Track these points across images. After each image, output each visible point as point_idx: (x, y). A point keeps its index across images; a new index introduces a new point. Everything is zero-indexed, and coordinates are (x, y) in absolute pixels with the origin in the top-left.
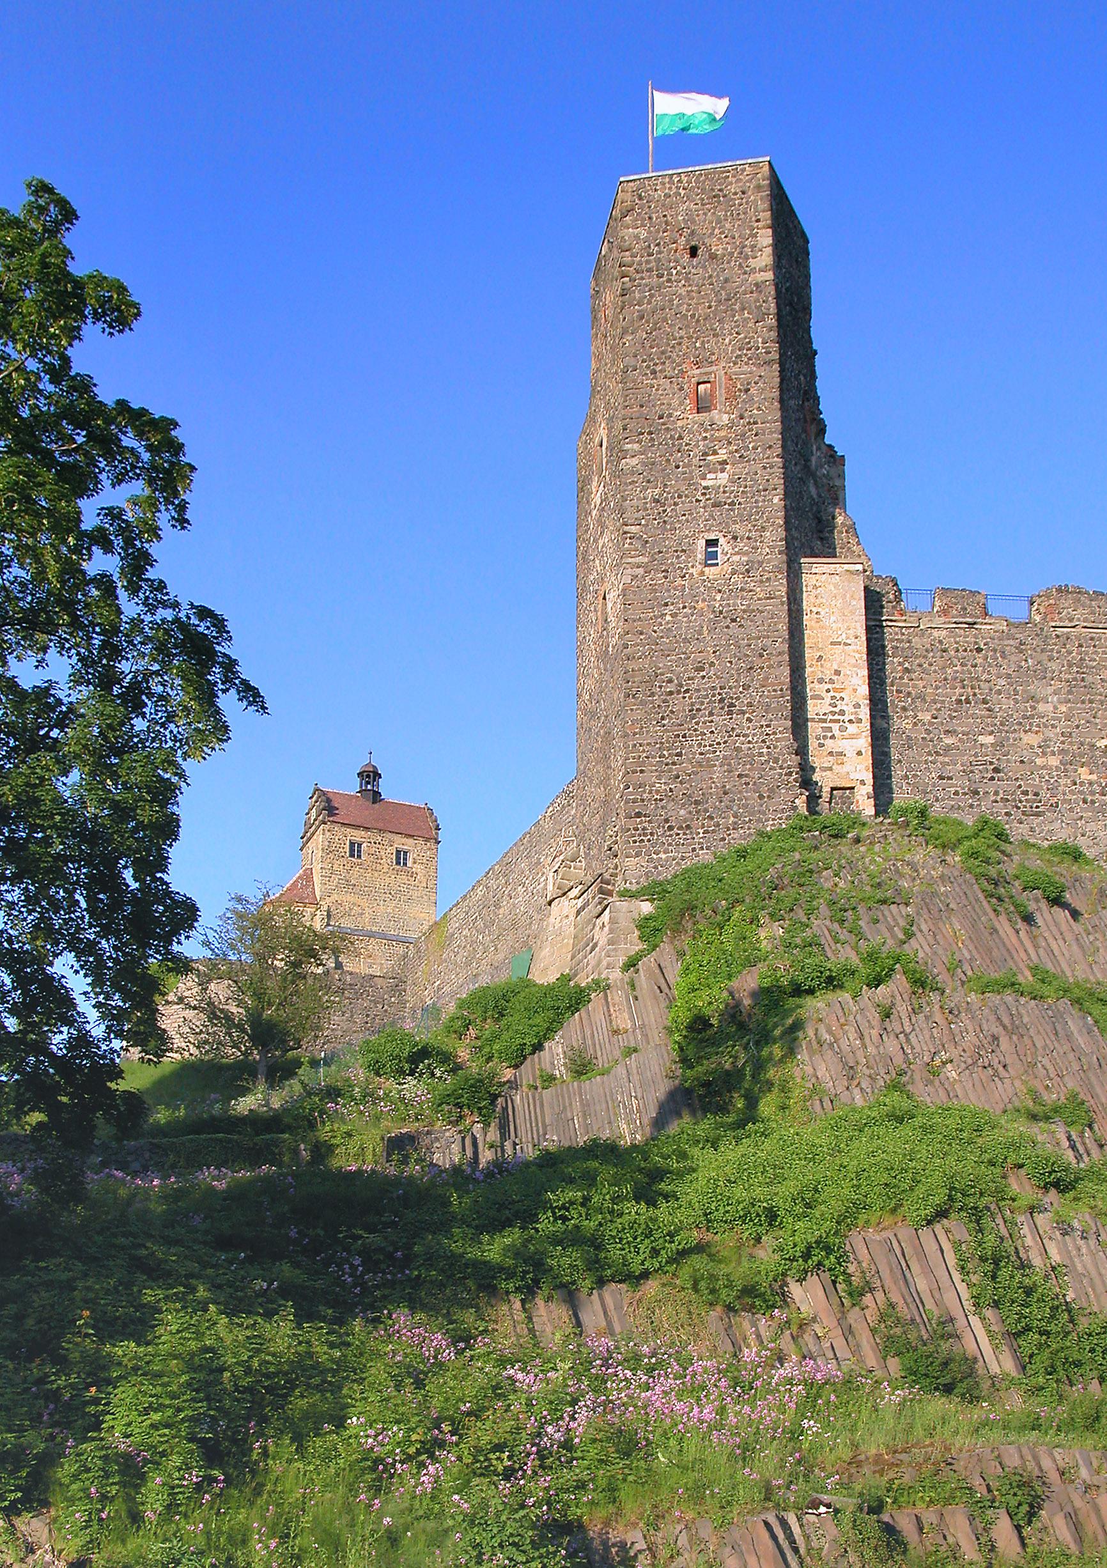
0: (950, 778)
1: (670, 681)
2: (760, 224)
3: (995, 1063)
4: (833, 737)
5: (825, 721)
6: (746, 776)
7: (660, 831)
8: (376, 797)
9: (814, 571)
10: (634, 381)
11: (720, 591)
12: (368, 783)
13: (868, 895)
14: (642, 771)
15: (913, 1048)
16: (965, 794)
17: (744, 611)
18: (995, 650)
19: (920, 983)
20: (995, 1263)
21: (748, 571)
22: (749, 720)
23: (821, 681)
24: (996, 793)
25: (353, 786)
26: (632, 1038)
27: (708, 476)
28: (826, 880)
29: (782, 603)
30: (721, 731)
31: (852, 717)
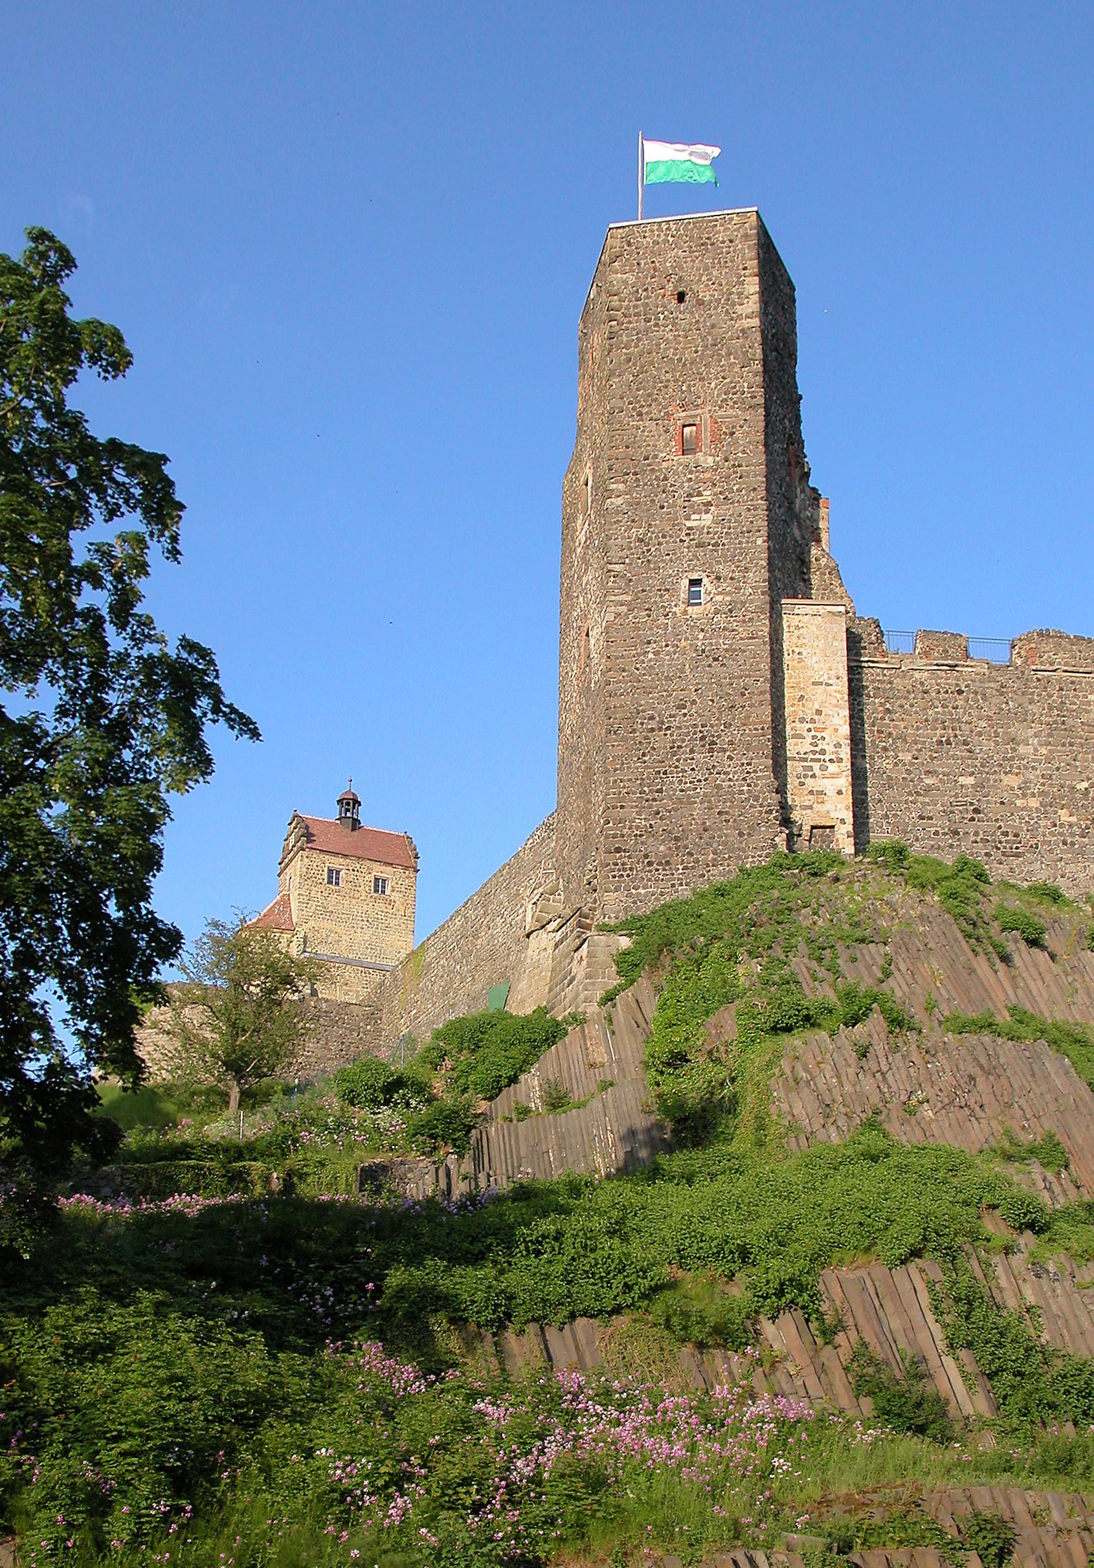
0: (930, 818)
1: (652, 718)
2: (747, 272)
3: (971, 1103)
4: (813, 776)
5: (806, 760)
6: (727, 813)
7: (640, 867)
8: (356, 824)
9: (796, 612)
10: (620, 422)
11: (702, 630)
12: (348, 810)
13: (846, 934)
14: (622, 807)
15: (889, 1087)
16: (945, 834)
17: (726, 650)
18: (976, 693)
19: (897, 1022)
20: (968, 1306)
21: (731, 611)
23: (802, 720)
24: (976, 834)
25: (332, 813)
26: (608, 1072)
27: (693, 517)
28: (804, 918)
29: (765, 643)
30: (702, 768)
31: (833, 757)
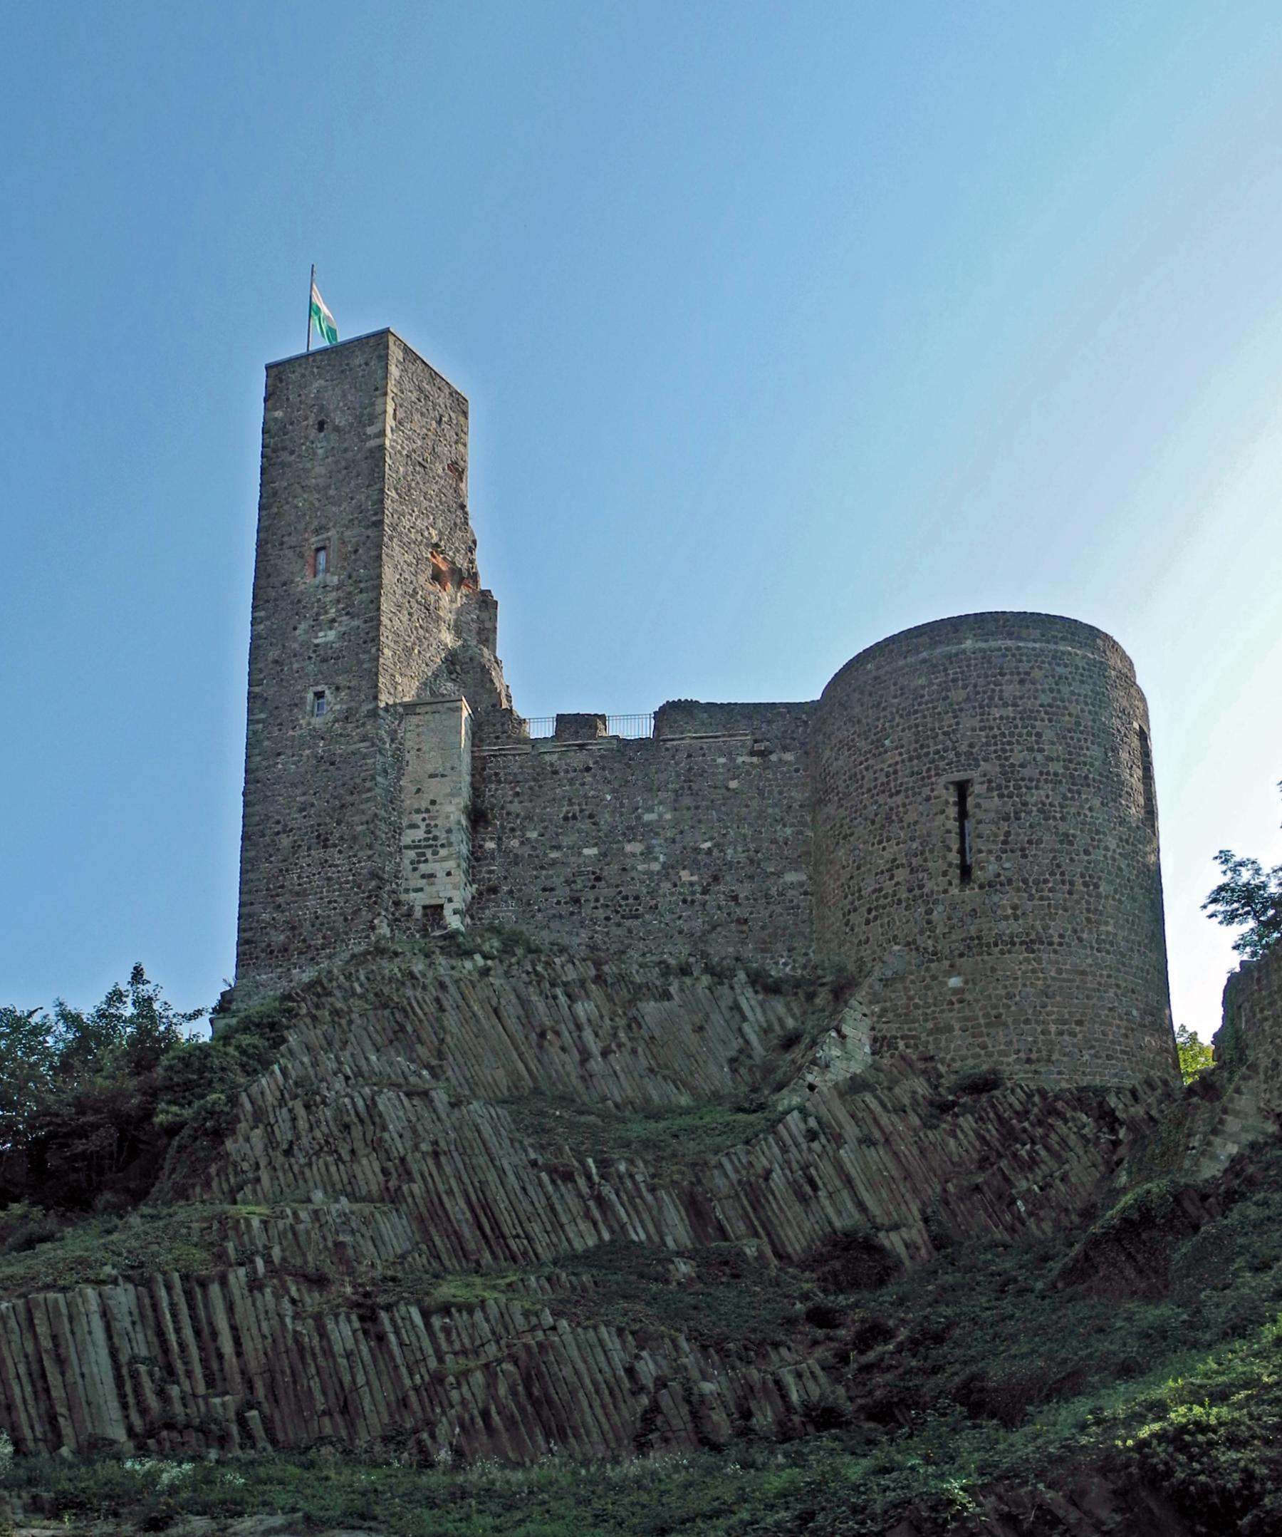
5: (419, 847)
22: (340, 852)
23: (418, 811)
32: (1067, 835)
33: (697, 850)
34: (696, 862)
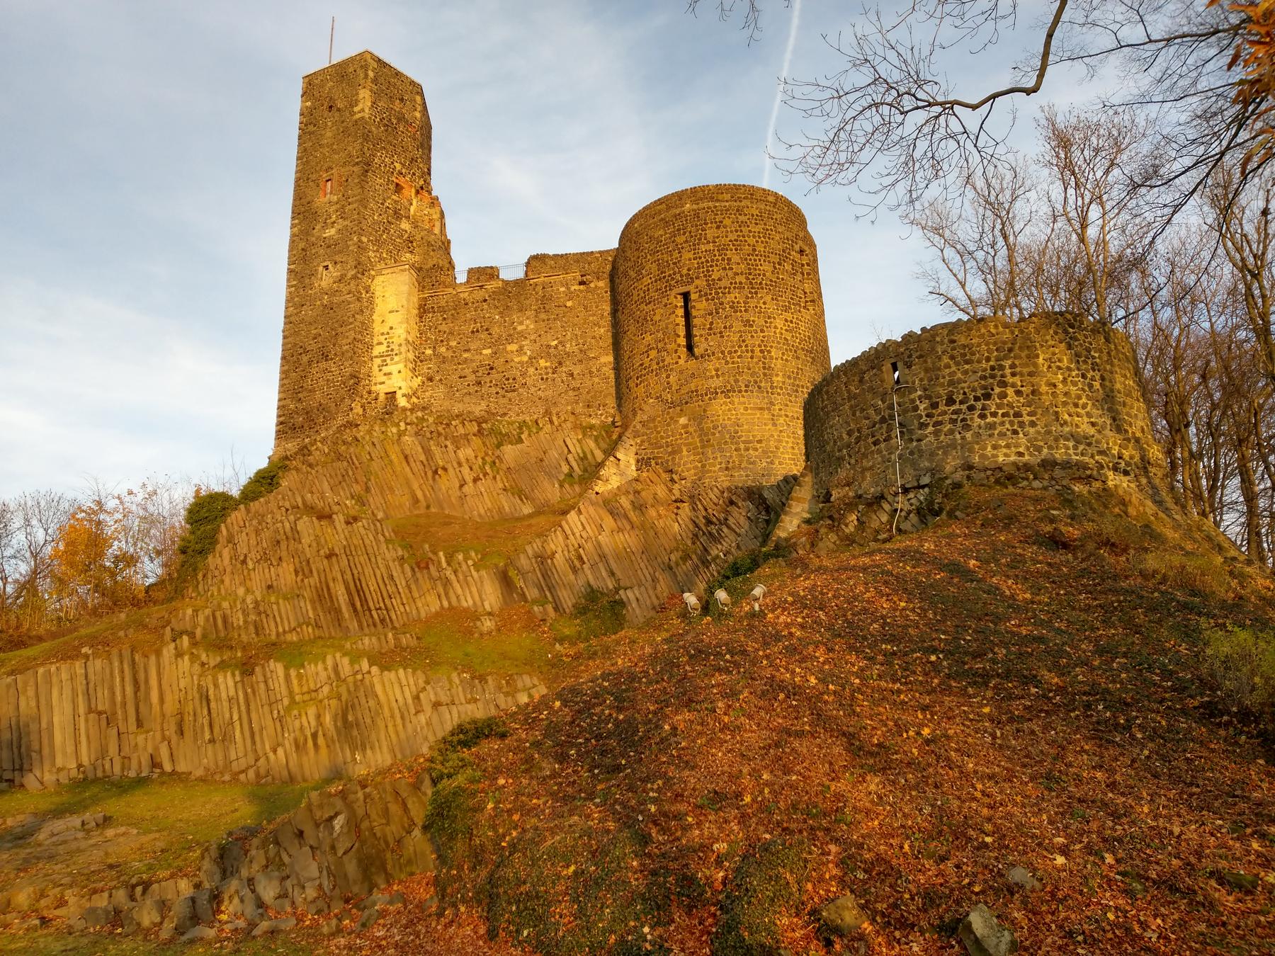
32: (748, 321)
33: (549, 346)
34: (548, 354)
